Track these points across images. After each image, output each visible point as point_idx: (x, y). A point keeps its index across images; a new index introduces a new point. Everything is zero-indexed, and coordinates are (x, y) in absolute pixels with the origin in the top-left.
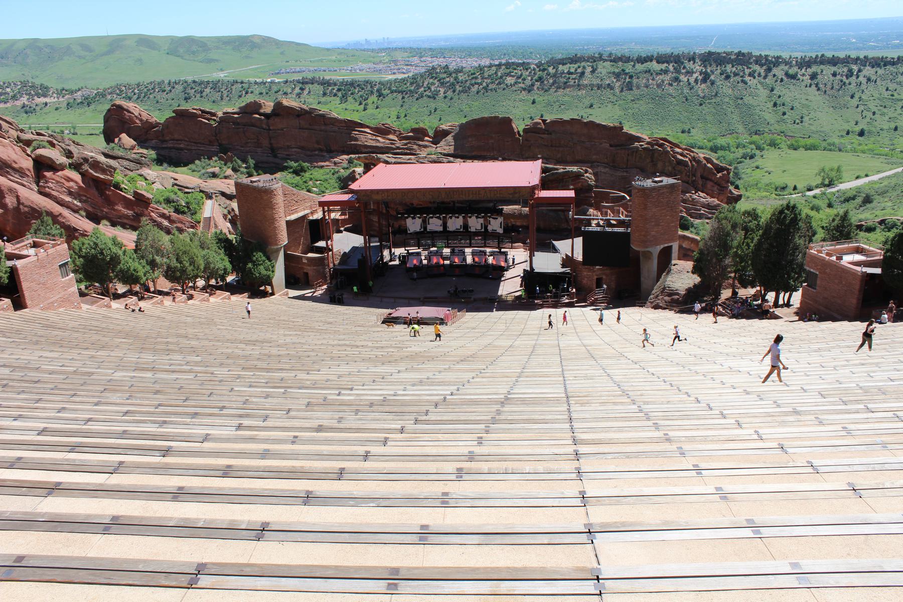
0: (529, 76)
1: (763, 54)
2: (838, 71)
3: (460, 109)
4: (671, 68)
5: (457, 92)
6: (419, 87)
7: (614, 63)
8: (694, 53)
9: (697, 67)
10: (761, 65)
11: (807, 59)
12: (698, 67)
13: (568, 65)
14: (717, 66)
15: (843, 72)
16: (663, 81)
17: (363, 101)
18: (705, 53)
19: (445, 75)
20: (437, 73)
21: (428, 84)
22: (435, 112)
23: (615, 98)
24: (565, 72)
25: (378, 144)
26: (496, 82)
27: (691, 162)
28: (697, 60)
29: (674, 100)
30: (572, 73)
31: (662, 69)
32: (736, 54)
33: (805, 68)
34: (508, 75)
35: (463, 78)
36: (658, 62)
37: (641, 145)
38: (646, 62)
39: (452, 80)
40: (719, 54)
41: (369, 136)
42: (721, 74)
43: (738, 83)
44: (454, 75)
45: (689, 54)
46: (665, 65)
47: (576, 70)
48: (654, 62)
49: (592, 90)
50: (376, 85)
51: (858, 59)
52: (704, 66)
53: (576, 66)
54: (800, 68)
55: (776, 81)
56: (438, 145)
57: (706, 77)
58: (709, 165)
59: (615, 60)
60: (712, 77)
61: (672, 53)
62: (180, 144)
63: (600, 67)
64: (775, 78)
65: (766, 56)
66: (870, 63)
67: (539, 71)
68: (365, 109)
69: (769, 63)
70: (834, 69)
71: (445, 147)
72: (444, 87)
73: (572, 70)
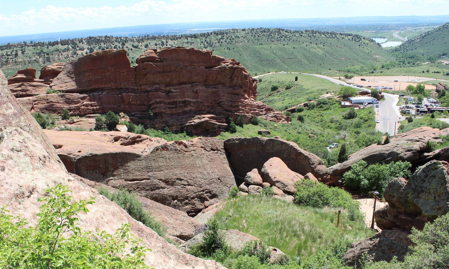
2: (158, 43)
4: (70, 47)
7: (34, 47)
8: (82, 38)
9: (86, 46)
10: (119, 42)
11: (141, 38)
12: (86, 46)
13: (5, 50)
14: (96, 45)
15: (160, 43)
16: (68, 55)
18: (88, 37)
28: (84, 41)
31: (65, 49)
32: (104, 37)
33: (141, 42)
36: (62, 45)
38: (55, 45)
42: (99, 49)
45: (78, 38)
47: (11, 53)
48: (60, 45)
49: (25, 64)
51: (164, 37)
52: (89, 45)
53: (11, 50)
54: (139, 42)
55: (129, 50)
59: (35, 45)
61: (69, 39)
63: (26, 50)
65: (120, 38)
66: (170, 38)
70: (155, 42)
71: (61, 85)
73: (9, 53)
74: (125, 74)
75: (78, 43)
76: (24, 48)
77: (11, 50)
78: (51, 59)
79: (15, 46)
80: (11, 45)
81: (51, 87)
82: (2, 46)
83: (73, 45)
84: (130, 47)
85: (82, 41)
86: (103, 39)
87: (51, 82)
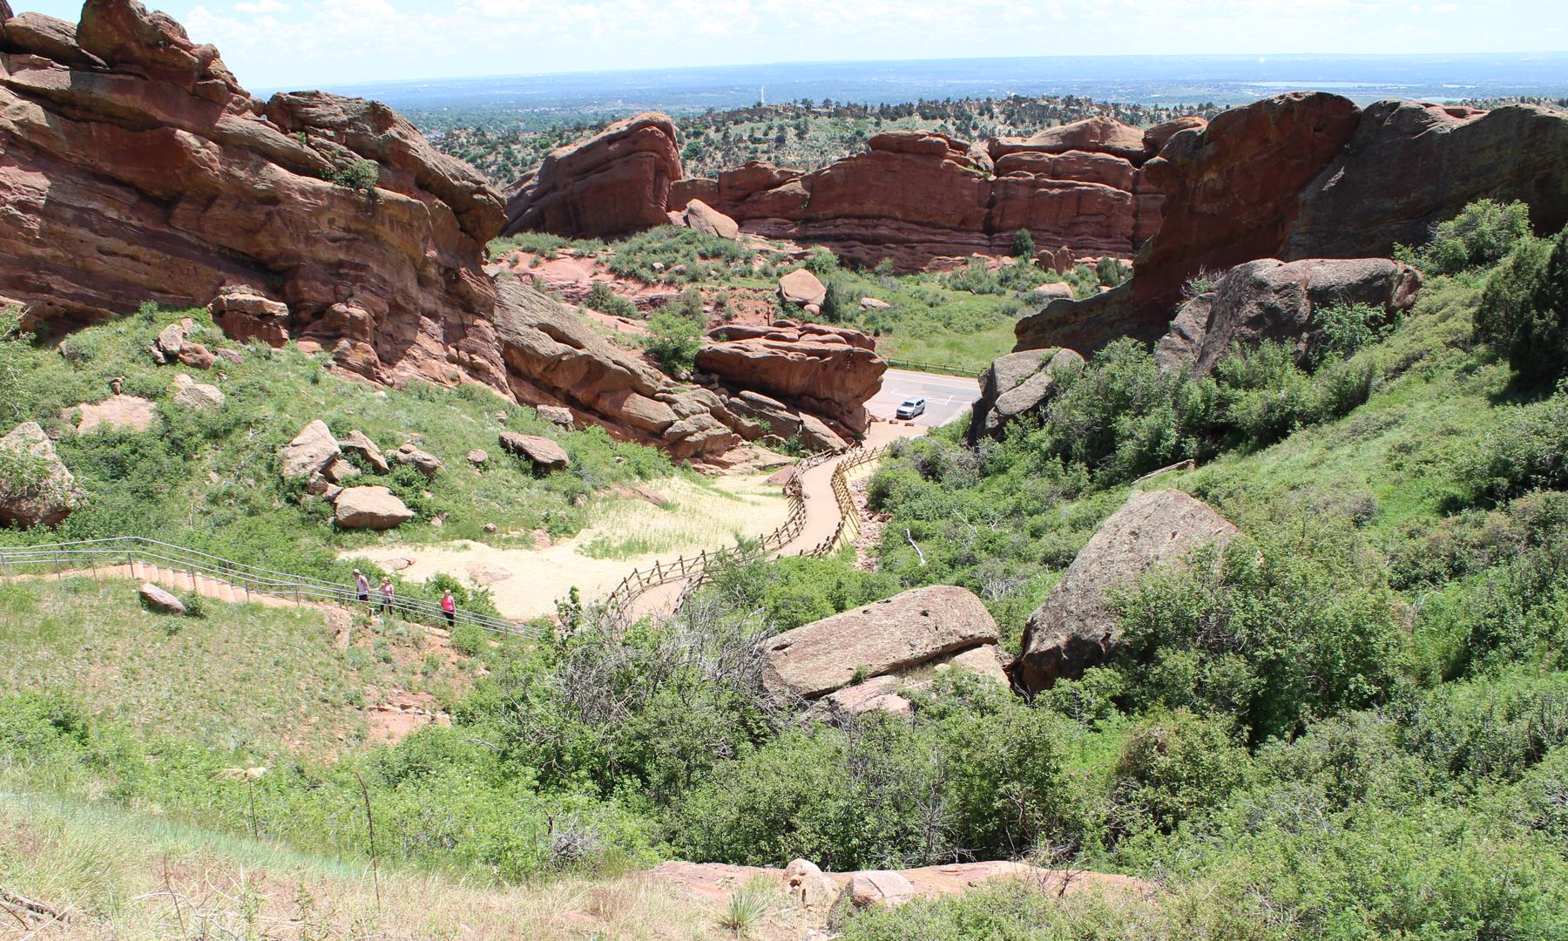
1: (1110, 101)
12: (1001, 127)
13: (747, 125)
14: (1034, 124)
19: (481, 150)
20: (461, 146)
28: (996, 110)
30: (758, 141)
35: (523, 154)
36: (925, 117)
38: (901, 116)
39: (500, 159)
44: (501, 149)
48: (917, 118)
52: (1011, 124)
53: (763, 126)
62: (875, 227)
63: (811, 127)
65: (1116, 106)
67: (688, 137)
73: (759, 135)
75: (975, 113)
76: (806, 121)
77: (763, 126)
80: (766, 110)
82: (739, 111)
83: (958, 122)
85: (990, 111)
86: (1060, 107)
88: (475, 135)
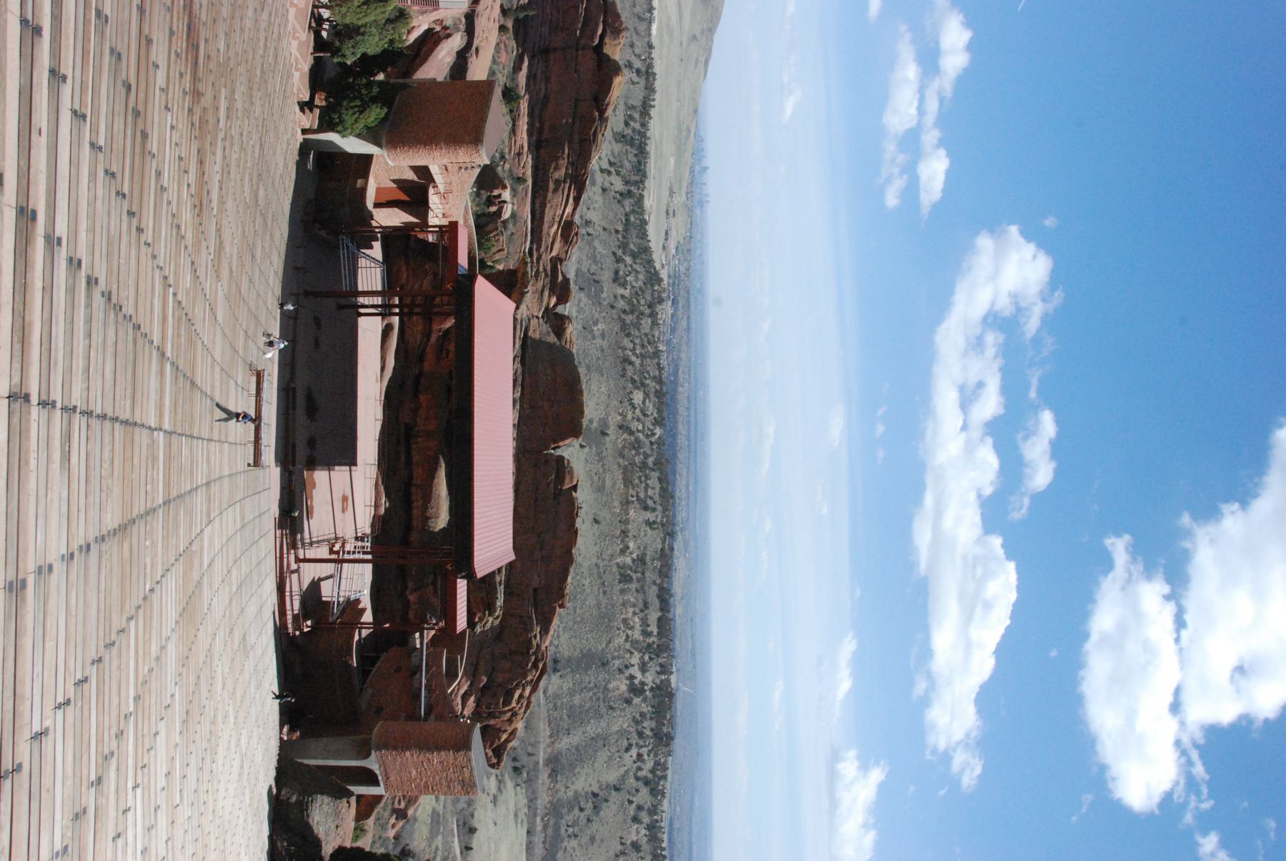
0: (644, 427)
1: (669, 773)
3: (598, 320)
4: (651, 640)
5: (623, 316)
6: (634, 256)
9: (650, 678)
10: (653, 771)
11: (660, 835)
13: (658, 486)
14: (652, 707)
16: (631, 628)
17: (614, 166)
21: (637, 272)
22: (594, 280)
23: (608, 558)
24: (648, 482)
25: (546, 226)
26: (635, 377)
27: (509, 710)
28: (663, 677)
29: (604, 646)
30: (646, 491)
33: (647, 833)
34: (647, 395)
35: (644, 325)
36: (659, 620)
37: (535, 636)
40: (670, 708)
41: (559, 212)
43: (628, 739)
46: (655, 631)
47: (651, 498)
50: (638, 189)
53: (657, 498)
56: (541, 320)
57: (636, 690)
58: (504, 736)
59: (666, 558)
60: (637, 700)
63: (655, 532)
64: (634, 791)
65: (665, 777)
67: (651, 443)
68: (602, 171)
69: (654, 784)
72: (631, 294)
73: (650, 492)
74: (541, 432)
75: (661, 660)
78: (626, 587)
79: (667, 510)
81: (537, 317)
83: (655, 646)
84: (637, 799)
87: (546, 323)
88: (659, 297)
